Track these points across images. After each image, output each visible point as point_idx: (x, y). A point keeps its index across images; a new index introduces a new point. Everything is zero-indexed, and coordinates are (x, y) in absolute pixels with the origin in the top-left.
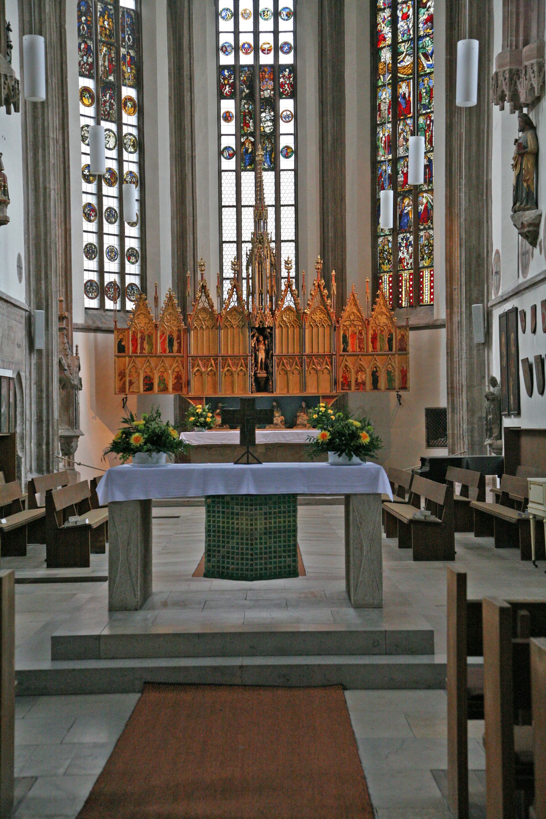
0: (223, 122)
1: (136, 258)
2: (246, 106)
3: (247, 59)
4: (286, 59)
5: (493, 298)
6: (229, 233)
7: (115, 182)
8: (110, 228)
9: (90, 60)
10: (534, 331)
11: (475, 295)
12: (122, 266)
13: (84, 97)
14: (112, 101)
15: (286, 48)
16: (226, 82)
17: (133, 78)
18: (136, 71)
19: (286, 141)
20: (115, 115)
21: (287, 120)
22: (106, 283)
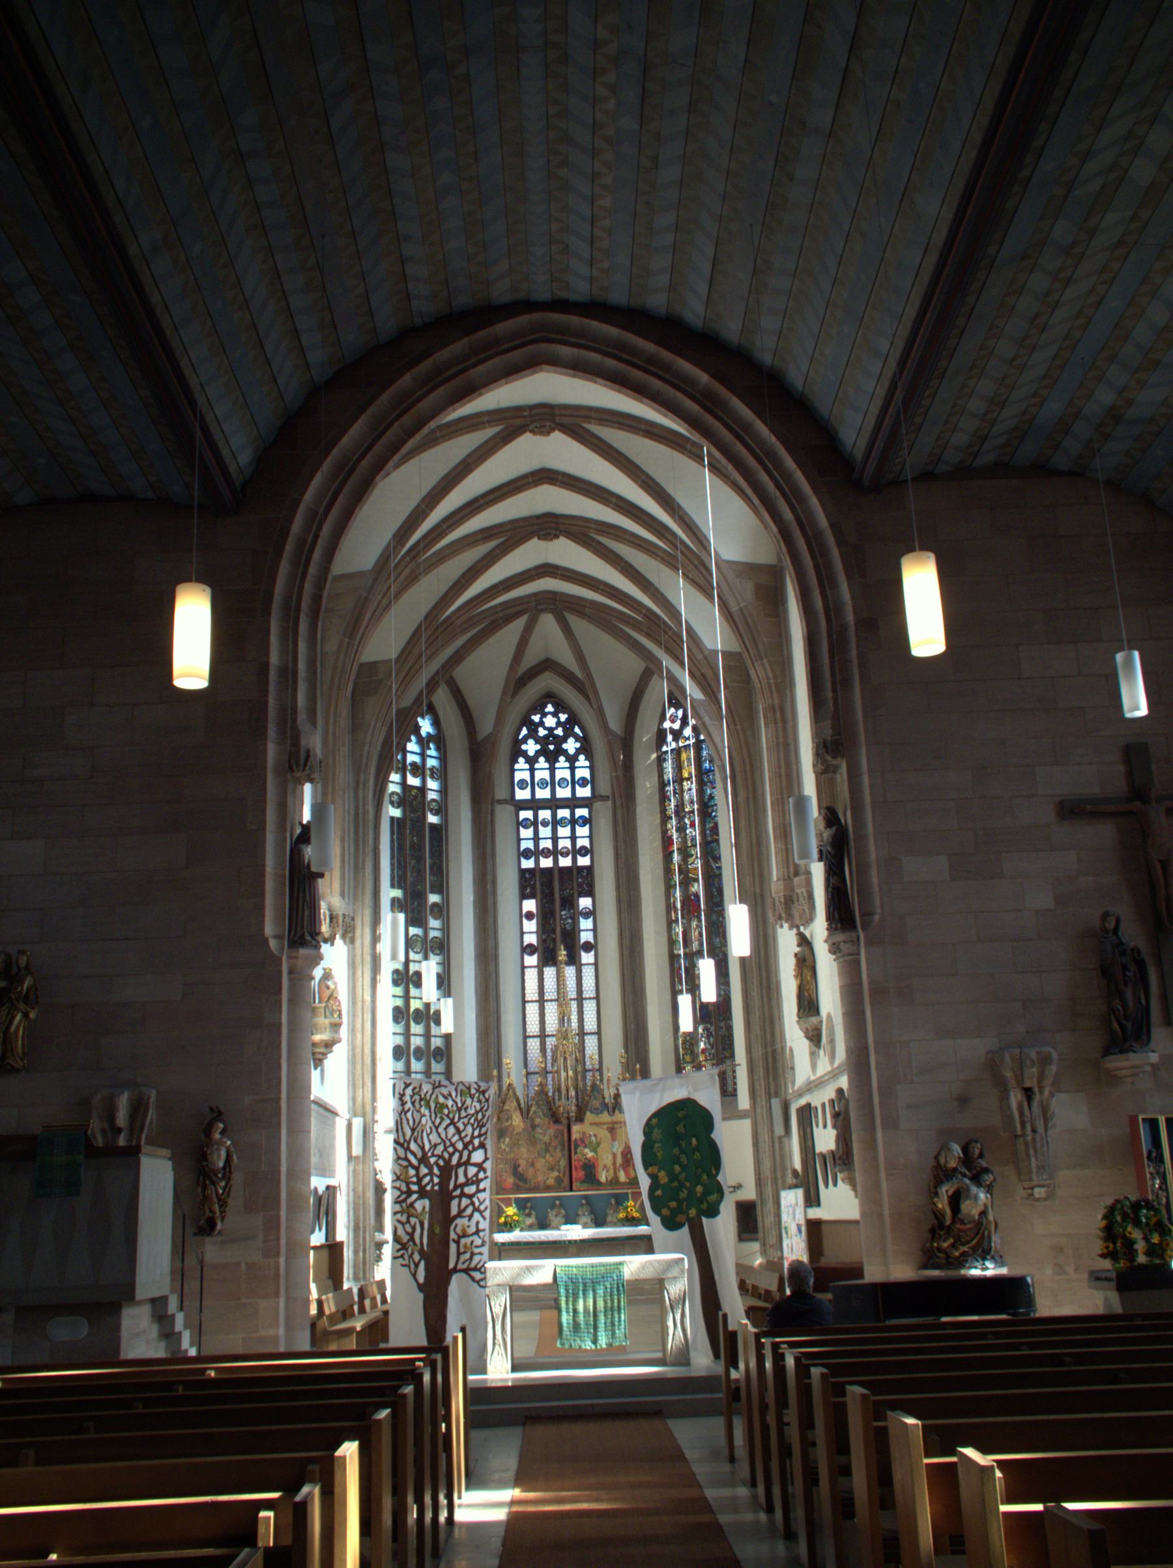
0: (524, 920)
3: (546, 863)
4: (583, 861)
5: (791, 1091)
6: (533, 1027)
8: (416, 1029)
10: (825, 1126)
11: (772, 1090)
12: (428, 1066)
19: (586, 937)
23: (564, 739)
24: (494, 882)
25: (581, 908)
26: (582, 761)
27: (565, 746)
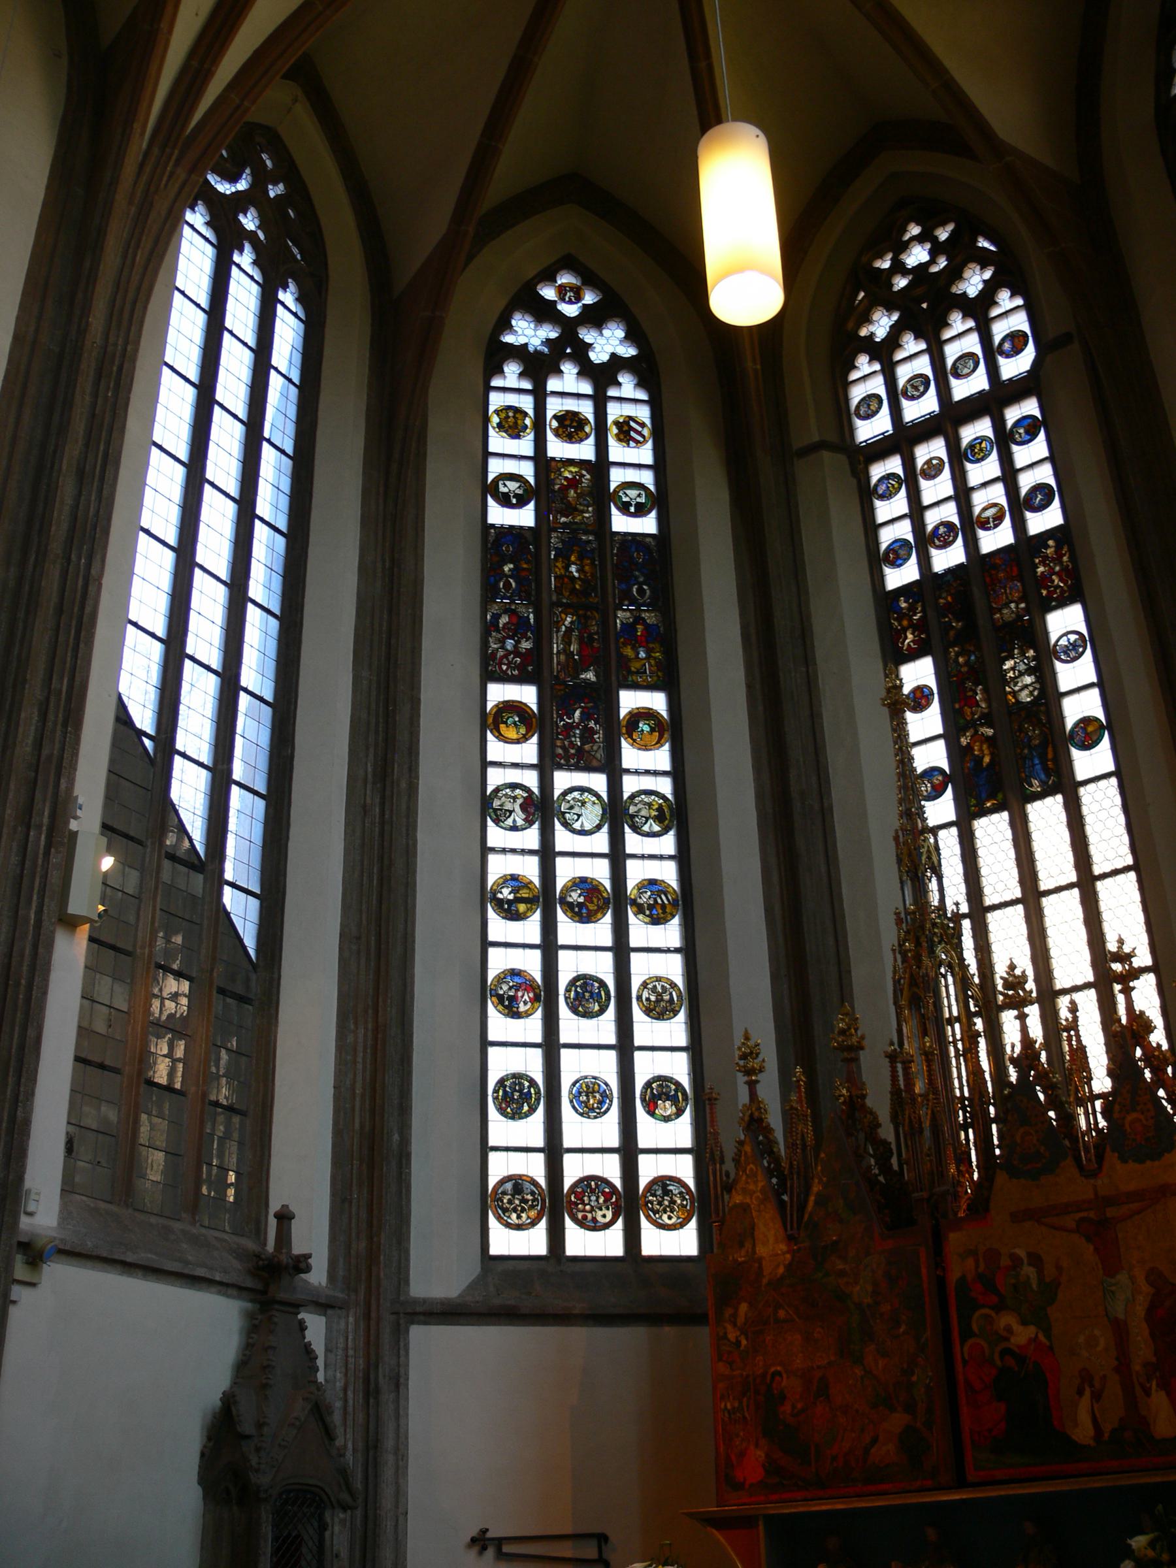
1: (674, 1100)
2: (961, 660)
3: (948, 558)
7: (602, 910)
9: (526, 645)
13: (506, 723)
14: (592, 724)
15: (1040, 497)
16: (905, 623)
17: (654, 669)
18: (663, 653)
20: (600, 754)
21: (1073, 654)
22: (568, 1183)
23: (955, 273)
24: (804, 634)
25: (1053, 638)
26: (1005, 300)
27: (959, 288)
